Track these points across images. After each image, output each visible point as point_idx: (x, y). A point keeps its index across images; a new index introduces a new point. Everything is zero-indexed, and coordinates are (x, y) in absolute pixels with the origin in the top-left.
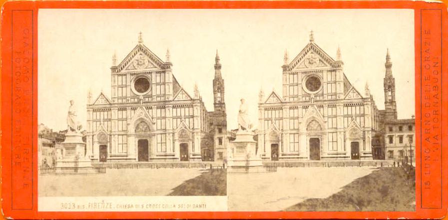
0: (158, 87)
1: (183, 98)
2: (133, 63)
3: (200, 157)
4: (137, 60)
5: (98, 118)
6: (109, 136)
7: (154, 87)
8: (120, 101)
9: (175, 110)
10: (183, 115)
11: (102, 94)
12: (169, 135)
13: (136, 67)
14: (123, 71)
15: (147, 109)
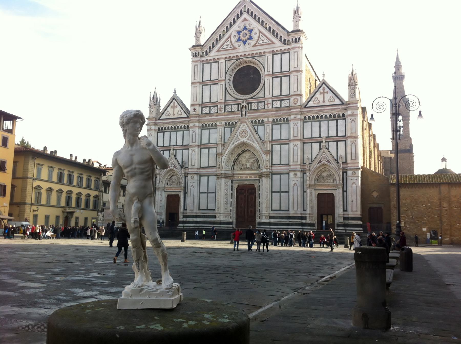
0: (277, 80)
1: (324, 102)
2: (230, 37)
3: (360, 222)
4: (239, 33)
5: (167, 144)
6: (183, 177)
7: (267, 81)
8: (206, 110)
9: (307, 125)
10: (324, 134)
11: (174, 99)
12: (295, 175)
13: (236, 45)
14: (213, 54)
15: (253, 126)
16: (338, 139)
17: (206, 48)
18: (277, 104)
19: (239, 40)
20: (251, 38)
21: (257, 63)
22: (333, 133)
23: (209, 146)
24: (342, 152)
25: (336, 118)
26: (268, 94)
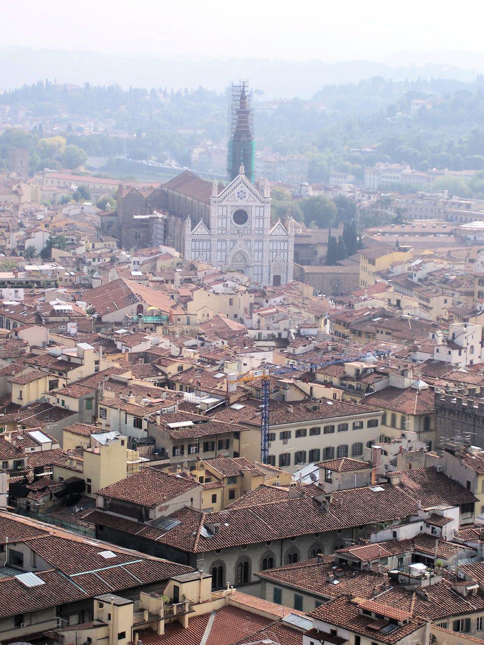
4: (239, 193)
5: (197, 248)
8: (220, 232)
13: (237, 199)
14: (224, 203)
16: (284, 251)
17: (221, 199)
18: (257, 232)
19: (238, 197)
20: (245, 197)
21: (246, 209)
22: (282, 248)
23: (221, 251)
24: (286, 257)
25: (284, 241)
26: (253, 227)
